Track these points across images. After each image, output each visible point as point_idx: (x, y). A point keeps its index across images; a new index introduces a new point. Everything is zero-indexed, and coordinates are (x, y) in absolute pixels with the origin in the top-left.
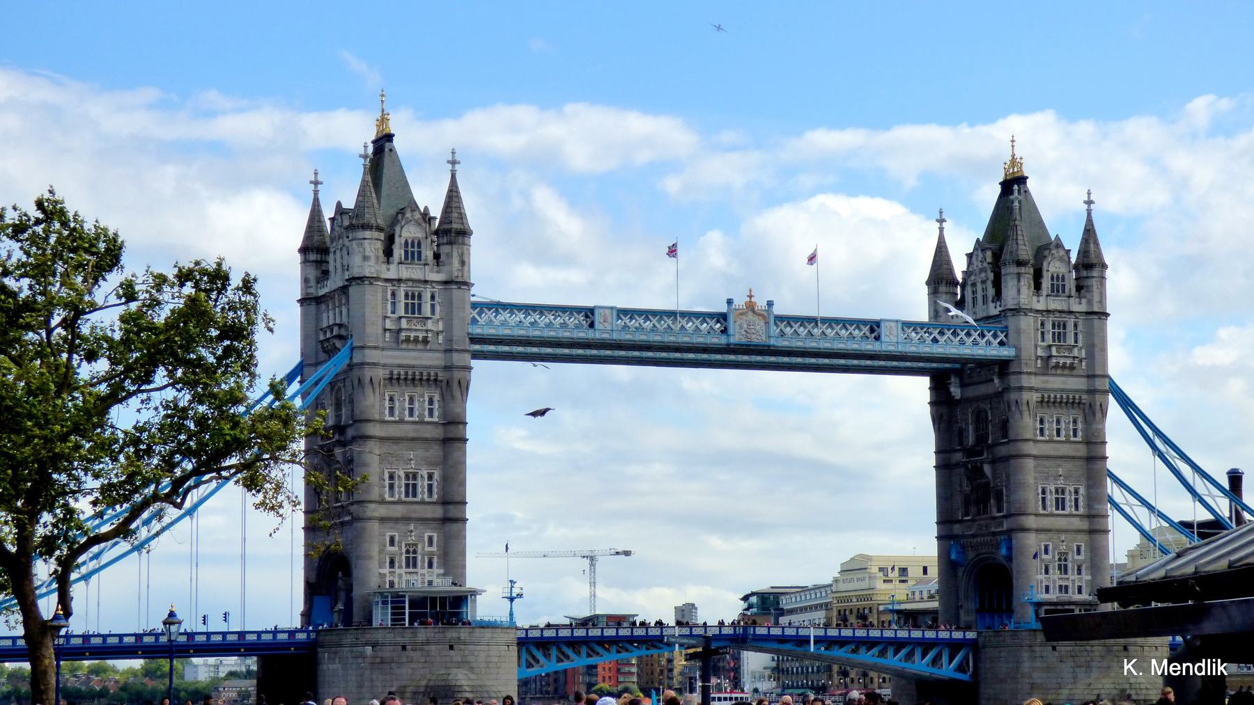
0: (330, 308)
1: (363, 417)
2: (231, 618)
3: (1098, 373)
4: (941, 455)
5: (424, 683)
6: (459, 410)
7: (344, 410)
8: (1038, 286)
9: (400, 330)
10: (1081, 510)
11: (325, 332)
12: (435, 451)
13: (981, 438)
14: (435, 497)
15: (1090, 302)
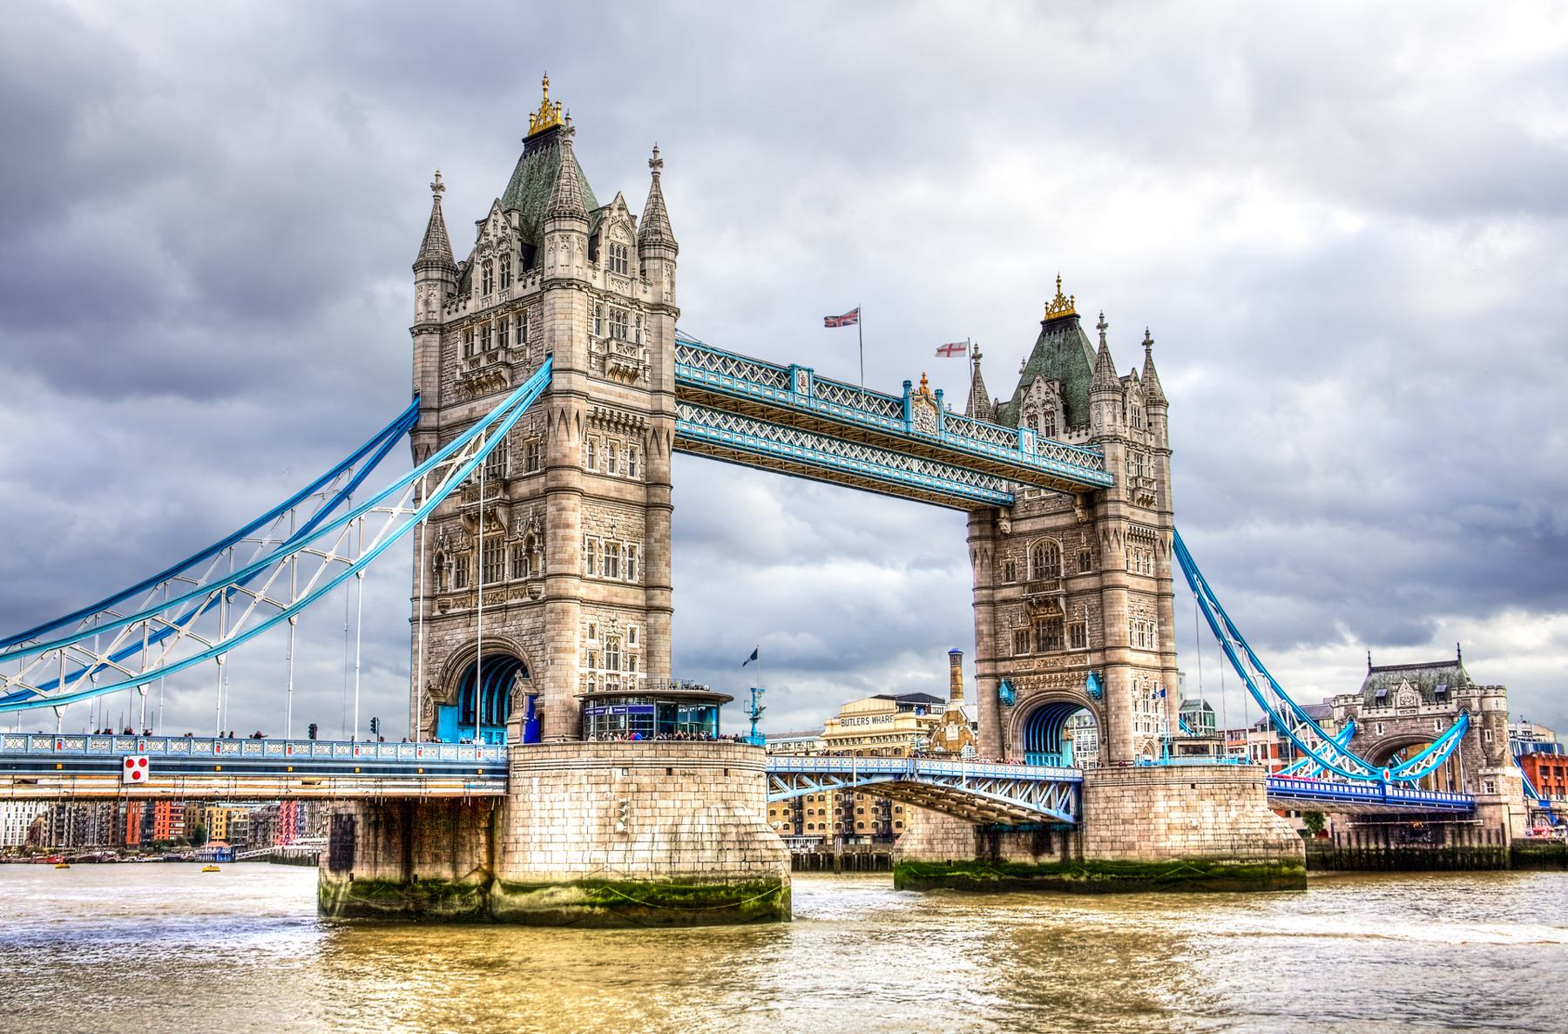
0: (476, 333)
1: (567, 463)
2: (381, 726)
3: (1168, 509)
4: (985, 592)
5: (703, 820)
6: (666, 469)
7: (509, 458)
8: (1124, 418)
9: (611, 355)
10: (1155, 648)
11: (477, 361)
12: (636, 520)
13: (1046, 570)
14: (636, 580)
15: (1158, 440)
